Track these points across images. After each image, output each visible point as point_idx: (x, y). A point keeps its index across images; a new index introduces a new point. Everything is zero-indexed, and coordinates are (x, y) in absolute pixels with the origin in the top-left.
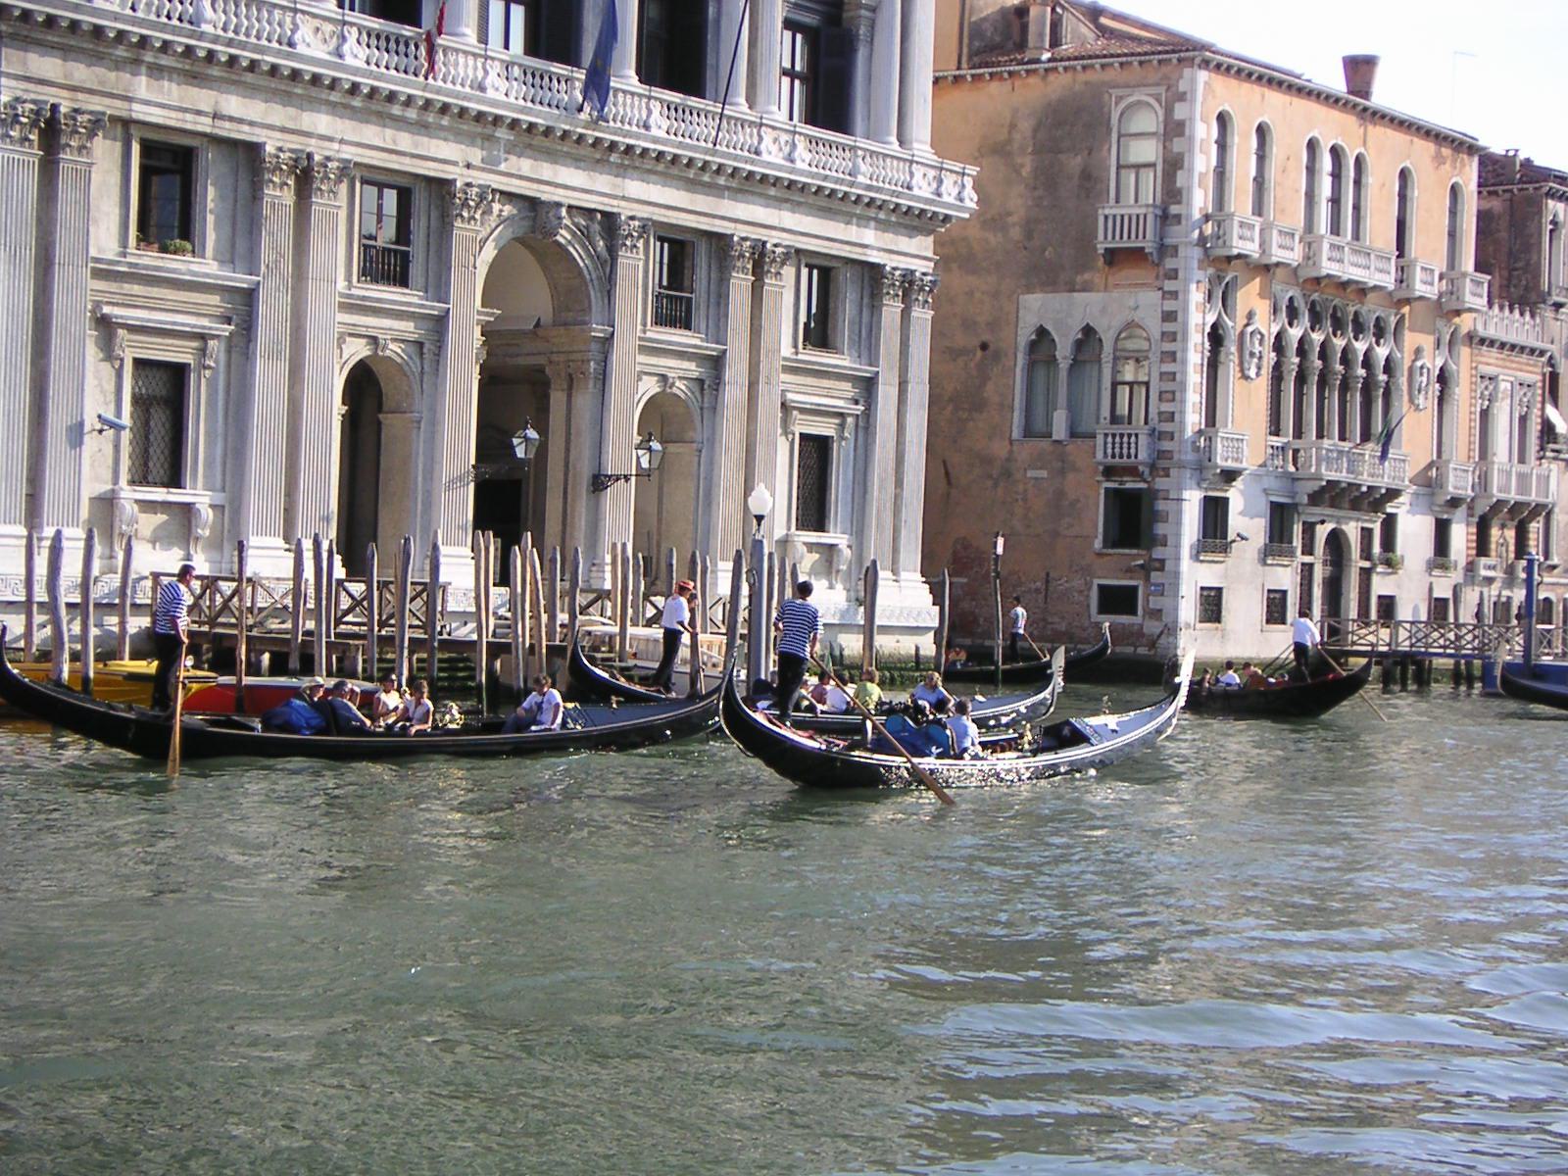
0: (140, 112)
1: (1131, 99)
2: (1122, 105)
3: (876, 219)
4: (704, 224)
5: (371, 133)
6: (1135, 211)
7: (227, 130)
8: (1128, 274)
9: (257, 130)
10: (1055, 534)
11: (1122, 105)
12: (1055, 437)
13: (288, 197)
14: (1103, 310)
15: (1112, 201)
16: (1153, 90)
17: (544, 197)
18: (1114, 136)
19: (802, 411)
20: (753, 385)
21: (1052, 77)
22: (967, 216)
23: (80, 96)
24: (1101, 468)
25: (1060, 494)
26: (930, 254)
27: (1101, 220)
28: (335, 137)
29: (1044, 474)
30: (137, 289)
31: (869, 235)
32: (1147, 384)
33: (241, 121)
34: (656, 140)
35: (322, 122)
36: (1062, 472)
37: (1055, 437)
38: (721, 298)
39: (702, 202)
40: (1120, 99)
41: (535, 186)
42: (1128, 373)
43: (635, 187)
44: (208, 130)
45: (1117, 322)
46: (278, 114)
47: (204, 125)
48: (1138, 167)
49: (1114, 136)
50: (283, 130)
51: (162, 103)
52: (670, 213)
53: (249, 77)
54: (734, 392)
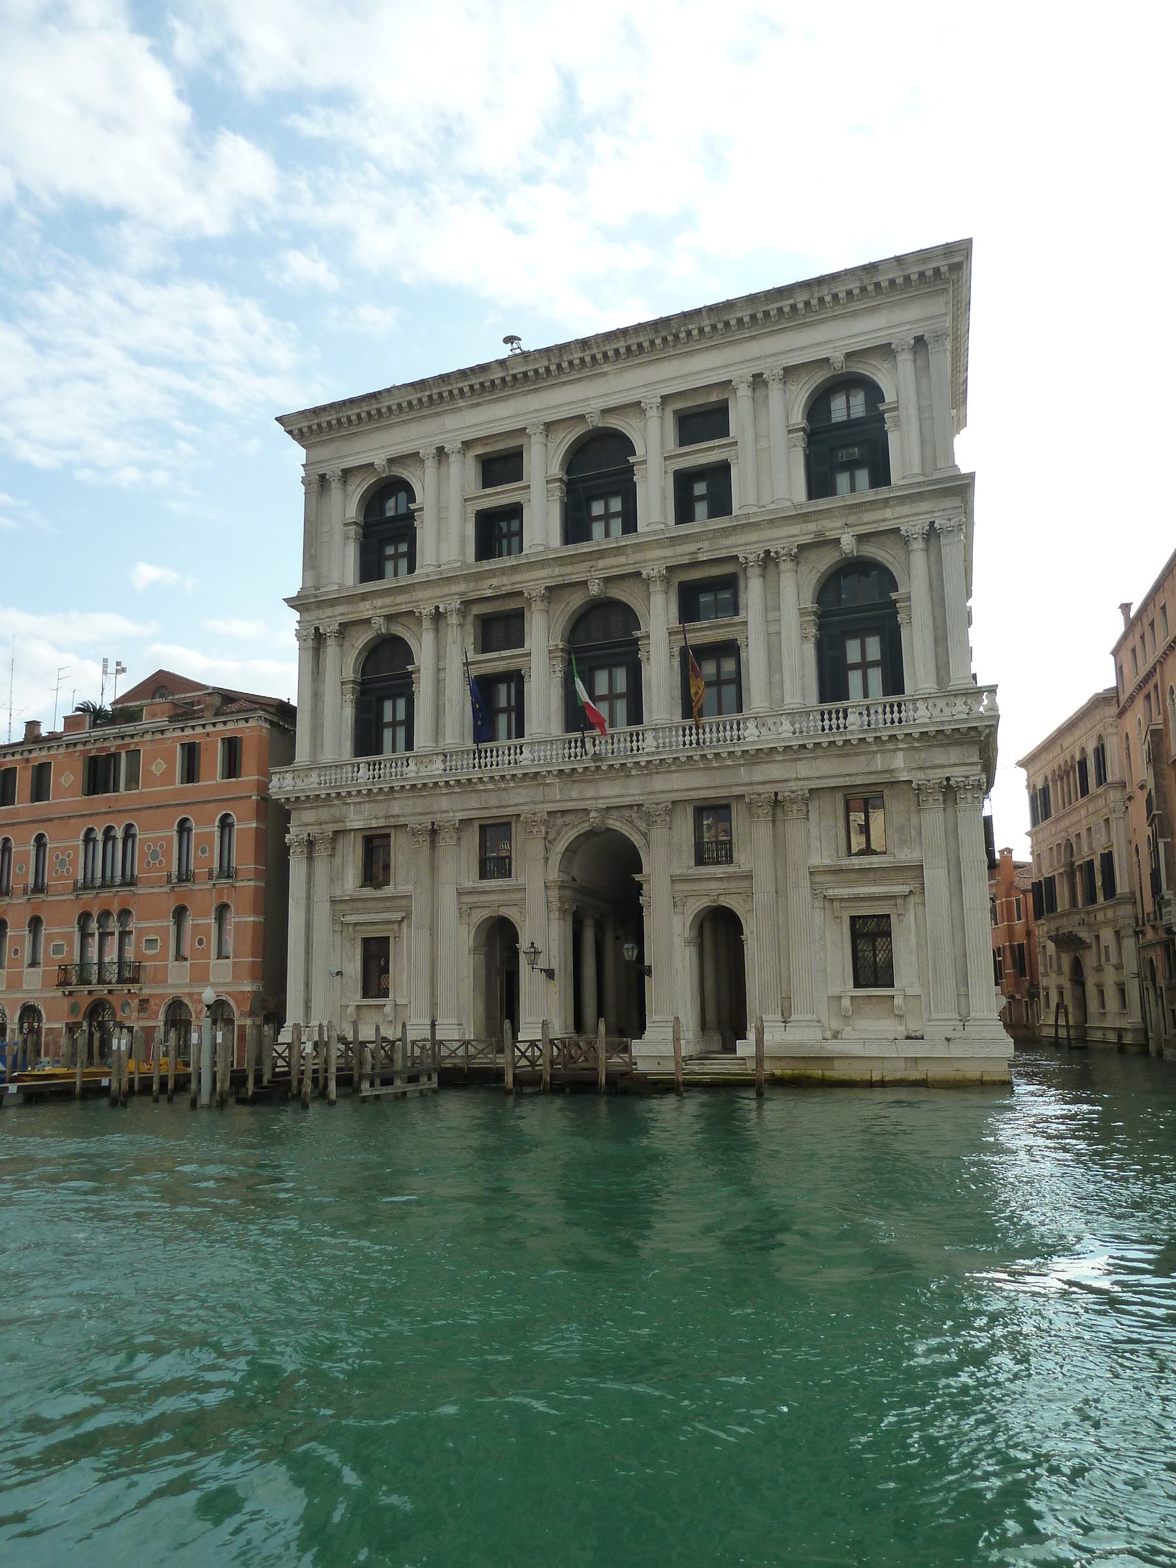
0: (350, 825)
4: (723, 793)
5: (472, 801)
7: (392, 822)
13: (427, 844)
19: (842, 900)
20: (780, 893)
26: (976, 759)
28: (450, 808)
30: (360, 905)
31: (899, 761)
33: (398, 816)
34: (648, 754)
35: (444, 803)
39: (720, 778)
41: (582, 803)
43: (659, 783)
46: (420, 805)
47: (382, 822)
50: (421, 814)
51: (358, 818)
52: (691, 793)
53: (397, 795)
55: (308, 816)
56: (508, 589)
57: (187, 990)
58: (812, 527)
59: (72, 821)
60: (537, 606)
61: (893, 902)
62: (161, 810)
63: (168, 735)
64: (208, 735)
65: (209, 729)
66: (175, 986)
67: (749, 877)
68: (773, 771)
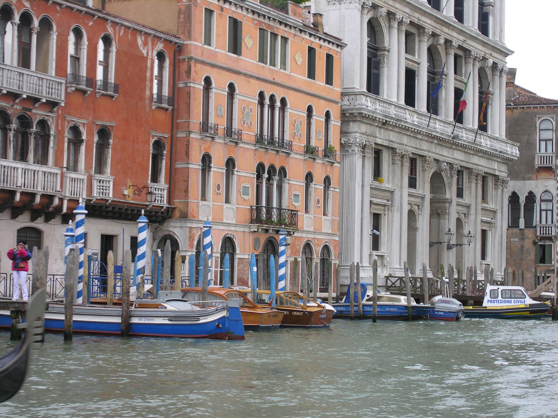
1: (543, 118)
2: (540, 120)
3: (497, 161)
6: (545, 155)
8: (544, 175)
9: (396, 145)
10: (522, 259)
11: (540, 120)
12: (520, 228)
14: (536, 186)
15: (538, 152)
16: (551, 116)
17: (441, 159)
18: (538, 130)
21: (515, 111)
22: (516, 159)
23: (369, 137)
24: (539, 238)
25: (522, 247)
26: (506, 171)
27: (536, 157)
29: (517, 240)
31: (495, 166)
32: (552, 211)
36: (523, 239)
37: (520, 228)
38: (470, 188)
40: (539, 118)
42: (543, 207)
44: (387, 145)
45: (542, 190)
47: (386, 143)
48: (546, 140)
49: (538, 130)
54: (472, 217)
55: (364, 128)
56: (421, 23)
57: (312, 236)
58: (483, 49)
59: (252, 80)
60: (426, 39)
61: (488, 225)
62: (299, 94)
63: (303, 35)
64: (321, 46)
65: (322, 42)
66: (308, 232)
67: (468, 207)
68: (476, 160)
